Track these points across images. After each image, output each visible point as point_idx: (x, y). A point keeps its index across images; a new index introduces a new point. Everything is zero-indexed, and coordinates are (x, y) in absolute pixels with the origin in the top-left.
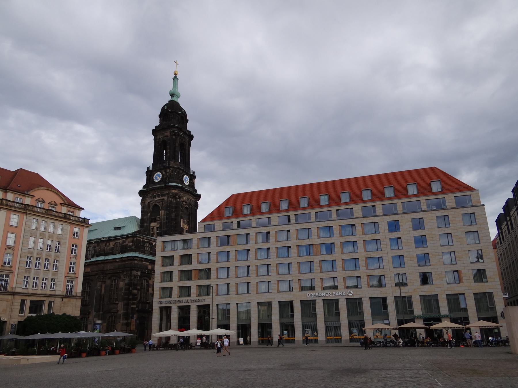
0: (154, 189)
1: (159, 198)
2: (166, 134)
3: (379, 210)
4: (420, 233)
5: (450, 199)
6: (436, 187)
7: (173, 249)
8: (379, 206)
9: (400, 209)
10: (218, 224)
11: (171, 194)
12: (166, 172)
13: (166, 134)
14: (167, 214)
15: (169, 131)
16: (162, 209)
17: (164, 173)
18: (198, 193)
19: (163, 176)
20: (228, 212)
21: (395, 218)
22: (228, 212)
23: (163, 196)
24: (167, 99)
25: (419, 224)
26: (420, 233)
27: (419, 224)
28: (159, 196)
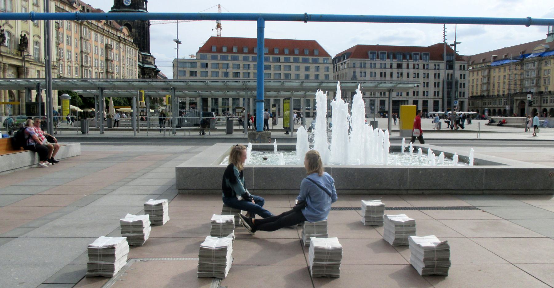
3: (292, 60)
4: (307, 73)
5: (321, 59)
6: (316, 52)
7: (184, 67)
8: (292, 58)
9: (301, 61)
10: (209, 55)
14: (139, 33)
16: (133, 28)
20: (214, 49)
21: (298, 64)
22: (214, 49)
25: (307, 69)
26: (307, 73)
27: (307, 69)
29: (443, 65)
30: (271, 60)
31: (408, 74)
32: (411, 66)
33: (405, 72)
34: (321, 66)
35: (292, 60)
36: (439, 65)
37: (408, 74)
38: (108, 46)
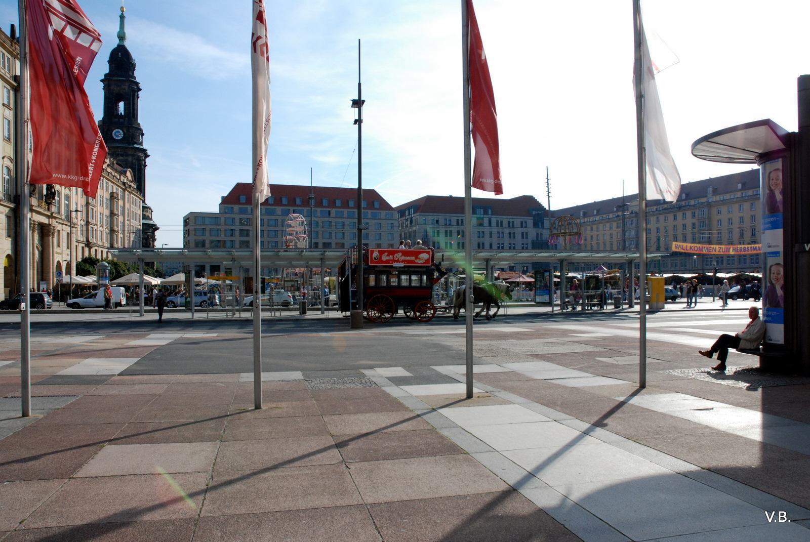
0: (118, 147)
1: (122, 158)
2: (123, 87)
3: (346, 215)
6: (377, 205)
10: (236, 208)
11: (136, 157)
12: (128, 131)
13: (123, 87)
15: (127, 84)
17: (125, 132)
18: (148, 154)
19: (124, 134)
22: (243, 199)
23: (127, 155)
24: (115, 42)
28: (122, 155)
29: (530, 222)
30: (319, 214)
31: (491, 233)
32: (494, 223)
33: (487, 230)
34: (384, 223)
35: (346, 215)
36: (526, 222)
37: (491, 233)
38: (115, 195)
